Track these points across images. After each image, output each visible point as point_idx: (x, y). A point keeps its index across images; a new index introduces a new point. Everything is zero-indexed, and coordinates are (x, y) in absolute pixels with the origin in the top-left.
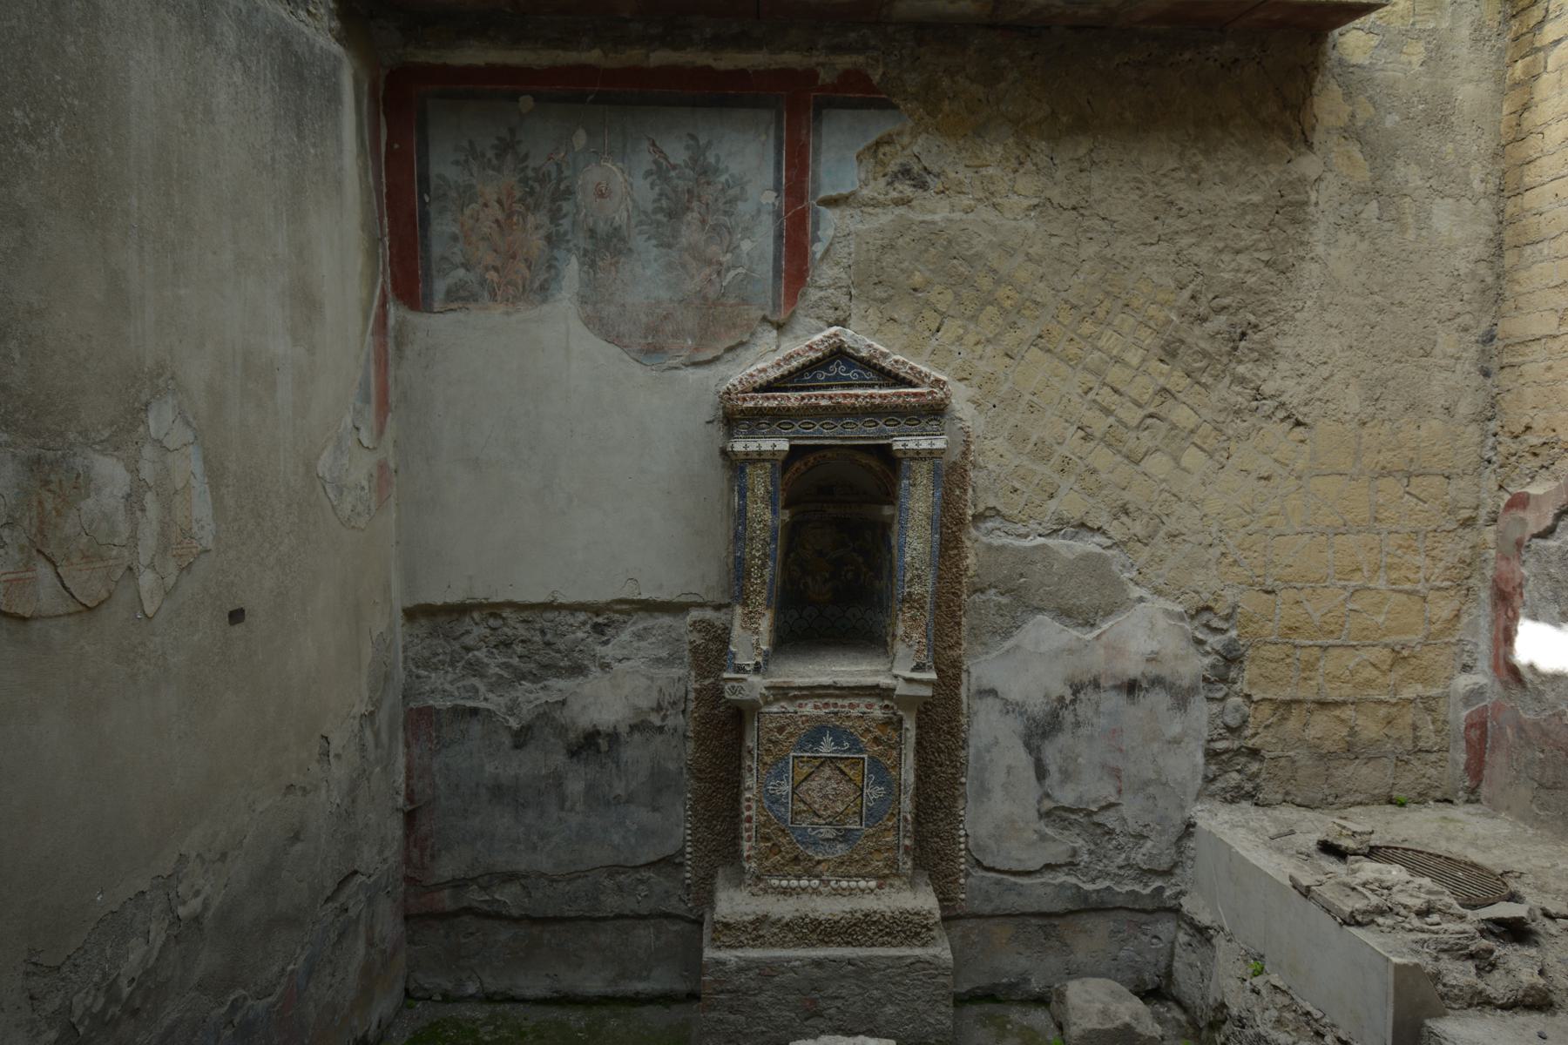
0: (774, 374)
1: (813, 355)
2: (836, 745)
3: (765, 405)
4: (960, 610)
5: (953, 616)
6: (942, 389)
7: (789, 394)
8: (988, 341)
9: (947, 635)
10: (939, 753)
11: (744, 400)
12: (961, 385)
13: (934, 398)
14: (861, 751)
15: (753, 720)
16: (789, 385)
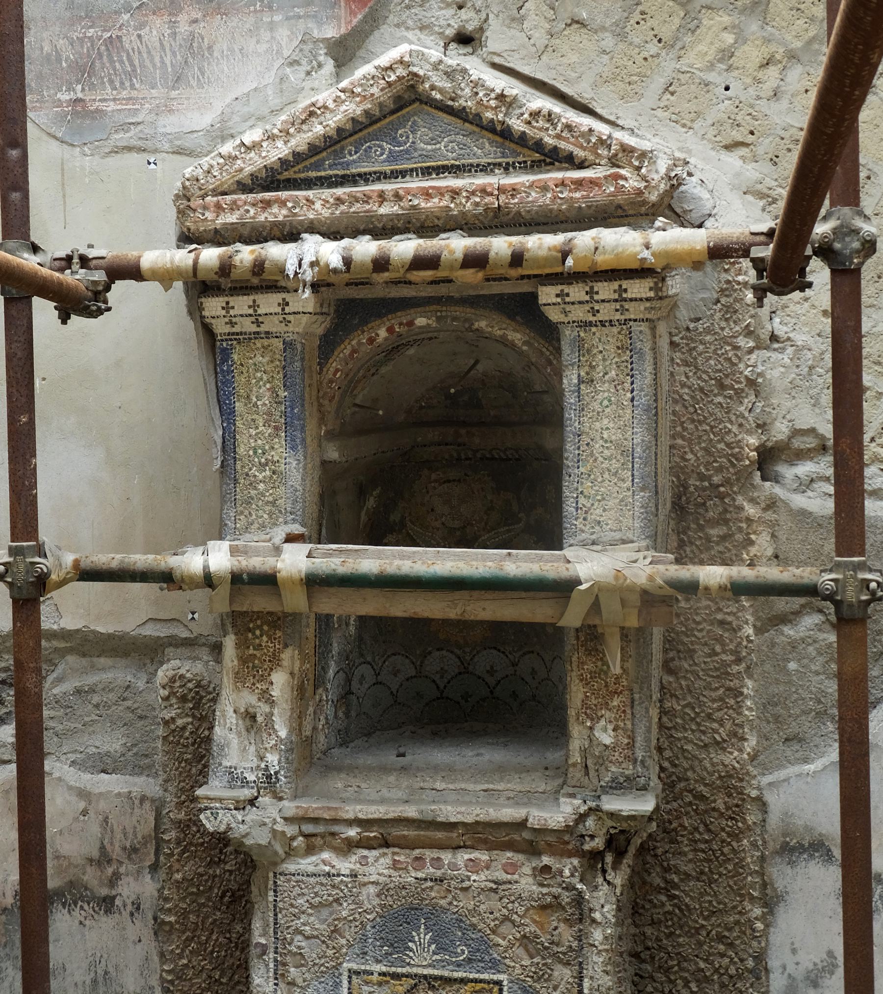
0: (280, 151)
1: (353, 108)
2: (441, 949)
3: (262, 218)
4: (738, 661)
5: (723, 673)
6: (638, 169)
7: (310, 194)
8: (793, 56)
9: (709, 716)
10: (697, 981)
11: (218, 207)
12: (732, 160)
13: (620, 189)
14: (495, 965)
15: (266, 887)
16: (313, 174)
